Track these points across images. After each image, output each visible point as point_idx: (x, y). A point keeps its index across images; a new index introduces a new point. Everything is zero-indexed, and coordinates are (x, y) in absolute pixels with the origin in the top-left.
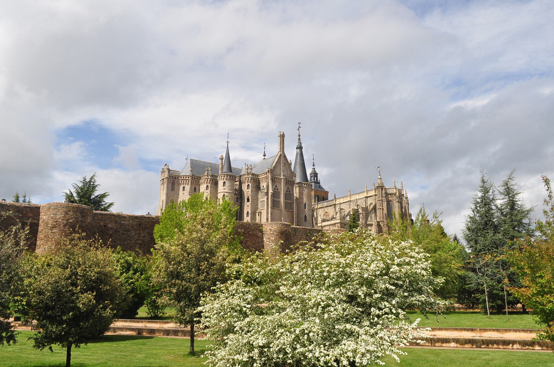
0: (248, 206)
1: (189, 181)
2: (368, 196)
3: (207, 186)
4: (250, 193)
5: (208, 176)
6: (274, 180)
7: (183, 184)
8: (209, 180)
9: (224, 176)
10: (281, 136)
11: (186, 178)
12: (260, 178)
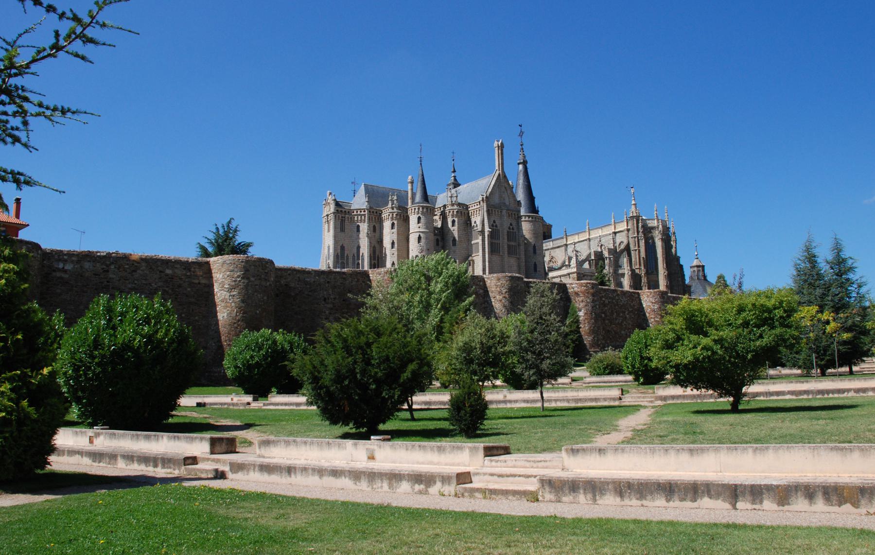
1: (365, 217)
2: (616, 231)
5: (393, 208)
6: (490, 212)
11: (361, 212)
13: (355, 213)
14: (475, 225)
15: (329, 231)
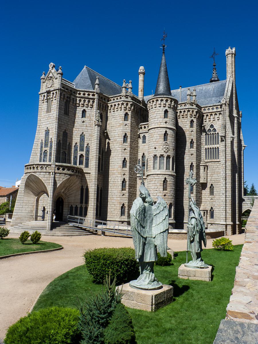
0: (192, 155)
1: (93, 102)
3: (126, 114)
4: (194, 133)
5: (126, 96)
8: (129, 104)
9: (167, 101)
10: (232, 54)
11: (89, 95)
12: (204, 112)
14: (212, 129)
15: (49, 110)
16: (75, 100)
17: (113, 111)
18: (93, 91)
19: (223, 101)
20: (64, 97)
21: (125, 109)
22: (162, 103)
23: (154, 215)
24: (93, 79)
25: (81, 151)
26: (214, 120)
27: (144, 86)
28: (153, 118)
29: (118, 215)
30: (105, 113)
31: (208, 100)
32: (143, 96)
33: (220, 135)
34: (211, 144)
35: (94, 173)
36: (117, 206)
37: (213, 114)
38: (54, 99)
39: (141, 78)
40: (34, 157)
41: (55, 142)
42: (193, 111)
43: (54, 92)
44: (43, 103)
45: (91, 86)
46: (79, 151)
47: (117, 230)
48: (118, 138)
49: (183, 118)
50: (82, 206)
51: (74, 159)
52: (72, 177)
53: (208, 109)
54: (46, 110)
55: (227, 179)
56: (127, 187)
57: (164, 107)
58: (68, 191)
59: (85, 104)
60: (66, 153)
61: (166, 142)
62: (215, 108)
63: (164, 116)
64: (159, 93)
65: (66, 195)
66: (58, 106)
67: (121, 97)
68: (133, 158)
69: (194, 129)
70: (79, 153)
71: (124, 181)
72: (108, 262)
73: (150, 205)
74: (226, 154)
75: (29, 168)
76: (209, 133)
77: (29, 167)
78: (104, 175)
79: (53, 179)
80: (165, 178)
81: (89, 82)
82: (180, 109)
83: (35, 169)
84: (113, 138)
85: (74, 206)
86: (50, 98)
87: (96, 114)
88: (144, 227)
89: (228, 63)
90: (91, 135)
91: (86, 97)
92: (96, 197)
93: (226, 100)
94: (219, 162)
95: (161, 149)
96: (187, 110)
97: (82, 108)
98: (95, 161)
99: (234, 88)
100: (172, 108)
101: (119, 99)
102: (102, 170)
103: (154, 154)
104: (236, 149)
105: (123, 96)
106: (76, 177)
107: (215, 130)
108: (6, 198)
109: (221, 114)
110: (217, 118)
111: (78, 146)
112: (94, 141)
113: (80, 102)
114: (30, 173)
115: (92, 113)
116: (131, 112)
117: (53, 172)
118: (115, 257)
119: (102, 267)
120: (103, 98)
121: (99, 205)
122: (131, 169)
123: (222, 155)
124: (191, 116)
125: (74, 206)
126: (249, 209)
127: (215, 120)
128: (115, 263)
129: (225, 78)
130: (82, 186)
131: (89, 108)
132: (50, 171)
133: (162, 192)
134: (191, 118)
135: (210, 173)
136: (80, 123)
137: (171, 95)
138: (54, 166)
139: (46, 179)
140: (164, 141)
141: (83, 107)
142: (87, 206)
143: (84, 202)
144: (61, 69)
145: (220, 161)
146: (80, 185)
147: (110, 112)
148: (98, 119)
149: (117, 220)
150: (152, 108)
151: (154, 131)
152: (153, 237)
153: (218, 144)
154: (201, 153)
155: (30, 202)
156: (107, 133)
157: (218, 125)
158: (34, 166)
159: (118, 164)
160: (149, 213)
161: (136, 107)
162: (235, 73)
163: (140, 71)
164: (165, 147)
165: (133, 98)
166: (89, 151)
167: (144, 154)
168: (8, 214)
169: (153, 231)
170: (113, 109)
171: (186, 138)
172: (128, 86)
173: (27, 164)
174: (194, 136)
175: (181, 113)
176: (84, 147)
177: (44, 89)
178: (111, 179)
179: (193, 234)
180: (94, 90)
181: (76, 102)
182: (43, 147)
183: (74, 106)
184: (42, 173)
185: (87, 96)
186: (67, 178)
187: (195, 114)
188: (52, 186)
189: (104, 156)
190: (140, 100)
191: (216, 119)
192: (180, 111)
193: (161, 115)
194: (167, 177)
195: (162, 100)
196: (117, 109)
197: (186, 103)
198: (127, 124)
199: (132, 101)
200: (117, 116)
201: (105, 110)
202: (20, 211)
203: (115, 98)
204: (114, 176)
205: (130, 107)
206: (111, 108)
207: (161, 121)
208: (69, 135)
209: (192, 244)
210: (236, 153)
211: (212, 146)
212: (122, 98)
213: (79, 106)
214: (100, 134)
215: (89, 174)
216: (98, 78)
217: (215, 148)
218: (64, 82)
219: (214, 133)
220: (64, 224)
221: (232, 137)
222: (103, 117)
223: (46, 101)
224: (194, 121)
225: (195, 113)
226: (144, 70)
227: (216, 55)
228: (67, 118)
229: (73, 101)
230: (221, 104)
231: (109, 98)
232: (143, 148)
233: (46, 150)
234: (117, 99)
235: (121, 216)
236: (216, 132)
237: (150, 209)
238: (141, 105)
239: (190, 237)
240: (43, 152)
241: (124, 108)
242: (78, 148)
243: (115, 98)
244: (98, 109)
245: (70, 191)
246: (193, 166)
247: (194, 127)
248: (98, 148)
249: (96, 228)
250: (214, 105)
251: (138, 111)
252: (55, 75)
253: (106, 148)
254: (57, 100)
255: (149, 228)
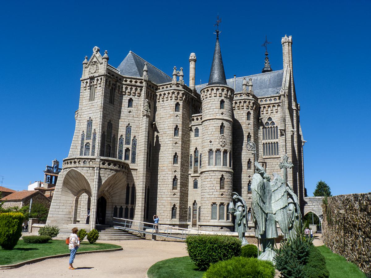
1: (141, 90)
3: (178, 104)
4: (251, 127)
5: (177, 85)
7: (130, 93)
9: (223, 90)
10: (289, 42)
11: (136, 82)
12: (261, 103)
13: (128, 82)
14: (270, 122)
15: (92, 98)
16: (121, 87)
17: (162, 101)
18: (140, 78)
19: (282, 91)
20: (110, 83)
21: (176, 98)
22: (218, 93)
23: (273, 191)
24: (140, 67)
25: (127, 144)
26: (272, 113)
27: (195, 74)
28: (207, 109)
29: (168, 217)
30: (153, 103)
31: (264, 91)
32: (195, 85)
33: (278, 129)
34: (269, 139)
35: (142, 170)
36: (167, 207)
37: (271, 106)
38: (98, 85)
39: (192, 65)
40: (73, 150)
41: (100, 133)
42: (249, 102)
43: (99, 78)
44: (85, 90)
45: (138, 73)
46: (125, 145)
47: (169, 234)
48: (168, 130)
49: (239, 109)
50: (128, 207)
51: (119, 153)
52: (119, 173)
53: (265, 100)
54: (88, 98)
55: (288, 177)
56: (179, 186)
57: (220, 96)
58: (112, 190)
59: (132, 92)
60: (110, 147)
61: (223, 135)
62: (273, 99)
63: (220, 106)
64: (214, 82)
65: (110, 194)
66: (103, 94)
67: (172, 85)
68: (185, 153)
69: (251, 121)
70: (125, 147)
71: (175, 179)
72: (216, 245)
73: (267, 181)
74: (286, 149)
75: (69, 163)
76: (267, 127)
77: (69, 161)
78: (151, 172)
79: (97, 175)
80: (222, 175)
81: (135, 69)
82: (235, 100)
83: (77, 163)
84: (161, 131)
85: (118, 207)
86: (93, 85)
87: (144, 103)
88: (264, 203)
89: (285, 52)
90: (138, 127)
91: (133, 85)
92: (144, 197)
93: (285, 91)
94: (279, 159)
95: (217, 143)
96: (244, 101)
97: (129, 96)
98: (143, 156)
99: (292, 79)
100: (229, 98)
101: (169, 87)
102: (149, 166)
103: (210, 148)
104: (296, 145)
105: (174, 84)
106: (122, 173)
107: (273, 123)
108: (22, 202)
109: (280, 106)
110: (276, 110)
111: (123, 138)
112: (142, 133)
113: (126, 90)
114: (70, 168)
115: (140, 102)
116: (182, 101)
117: (97, 167)
118: (222, 240)
119: (208, 252)
120: (152, 86)
121: (146, 206)
122: (182, 165)
123: (281, 150)
124: (248, 108)
125: (118, 207)
126: (311, 211)
127: (273, 113)
128: (222, 247)
129: (281, 67)
130: (128, 184)
131: (136, 97)
132: (94, 166)
133: (219, 191)
134: (247, 110)
135: (270, 171)
136: (126, 113)
137: (226, 84)
138: (99, 160)
139: (89, 175)
140: (220, 134)
141: (129, 95)
142: (134, 207)
143: (130, 202)
144: (107, 53)
145: (280, 158)
146: (126, 183)
147: (158, 102)
148: (146, 109)
149: (167, 223)
150: (206, 98)
151: (209, 123)
152: (274, 213)
153: (277, 138)
154: (258, 148)
155: (68, 202)
156: (155, 124)
157: (276, 118)
158: (76, 160)
159: (168, 160)
160: (268, 189)
161: (187, 96)
162: (292, 62)
163: (190, 58)
164: (221, 140)
165: (184, 87)
166: (136, 145)
167: (196, 149)
168: (32, 219)
169: (272, 207)
170: (162, 99)
171: (242, 131)
172: (179, 74)
173: (66, 158)
174: (251, 130)
175: (236, 104)
176: (130, 140)
177: (86, 74)
178: (161, 176)
179: (292, 220)
180: (141, 76)
181: (122, 90)
182: (85, 139)
183: (119, 94)
184: (84, 168)
185: (134, 83)
186: (113, 174)
187: (252, 105)
188: (97, 182)
189: (151, 151)
190: (192, 89)
191: (274, 111)
192: (236, 102)
193: (216, 105)
194: (224, 173)
195: (217, 90)
196: (166, 98)
197: (242, 93)
198: (178, 115)
199: (184, 90)
200: (167, 106)
201: (153, 99)
202: (56, 213)
203: (165, 87)
204: (163, 173)
205: (181, 96)
206: (160, 97)
207: (216, 112)
208: (113, 126)
209: (291, 231)
210: (296, 149)
211: (270, 141)
212: (173, 86)
213: (125, 95)
214: (149, 126)
215: (136, 171)
216: (146, 65)
217: (274, 143)
218: (109, 67)
219: (272, 126)
220: (108, 227)
221: (293, 131)
222: (151, 107)
223: (89, 88)
224: (250, 113)
225: (251, 104)
226: (195, 57)
227: (268, 43)
228: (112, 107)
229: (119, 88)
230: (280, 95)
231: (158, 86)
232: (195, 142)
233: (88, 143)
234: (167, 87)
235: (172, 219)
236: (275, 126)
237: (268, 186)
238: (192, 95)
239: (289, 223)
240: (85, 144)
241: (175, 97)
242: (123, 140)
243: (164, 86)
244: (146, 98)
245: (114, 190)
246: (251, 162)
247: (251, 119)
248: (147, 141)
249: (144, 231)
250: (272, 96)
251: (190, 100)
252: (100, 59)
253: (155, 142)
254: (102, 87)
255: (269, 204)
